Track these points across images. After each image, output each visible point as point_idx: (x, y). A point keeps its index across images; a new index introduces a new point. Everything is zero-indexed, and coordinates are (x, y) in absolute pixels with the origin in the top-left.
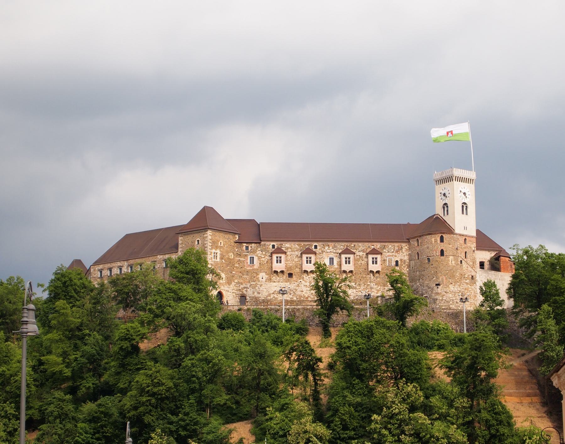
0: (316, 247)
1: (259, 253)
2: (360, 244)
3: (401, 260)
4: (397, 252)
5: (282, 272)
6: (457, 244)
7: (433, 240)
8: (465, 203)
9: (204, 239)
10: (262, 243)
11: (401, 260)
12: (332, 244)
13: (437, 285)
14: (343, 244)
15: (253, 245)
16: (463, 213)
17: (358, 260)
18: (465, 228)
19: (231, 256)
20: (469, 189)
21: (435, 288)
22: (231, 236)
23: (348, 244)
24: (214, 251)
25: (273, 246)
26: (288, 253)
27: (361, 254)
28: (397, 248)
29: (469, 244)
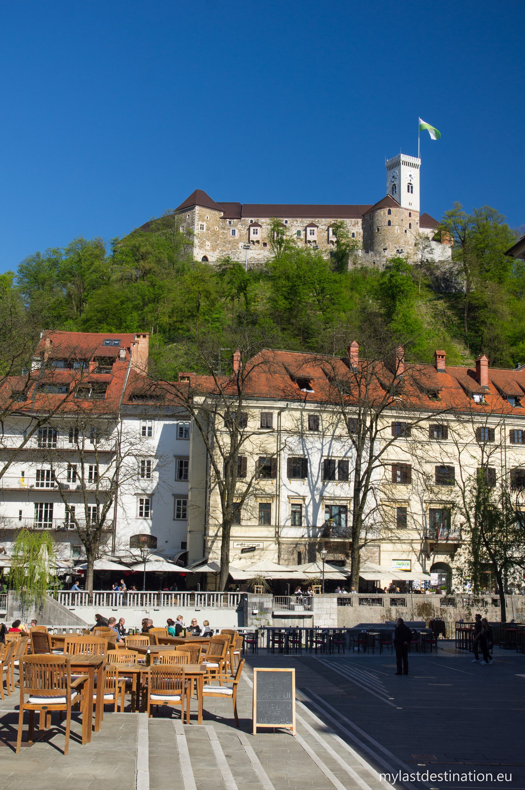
0: (286, 222)
1: (239, 226)
2: (323, 220)
3: (357, 232)
4: (353, 225)
5: (258, 242)
6: (403, 217)
7: (382, 213)
8: (410, 184)
9: (193, 213)
10: (242, 219)
11: (357, 232)
12: (299, 220)
13: (384, 249)
14: (309, 219)
15: (235, 220)
16: (408, 191)
17: (321, 232)
18: (410, 204)
19: (216, 228)
20: (416, 173)
21: (383, 252)
22: (217, 213)
23: (313, 219)
24: (200, 223)
25: (251, 221)
26: (263, 227)
27: (324, 227)
28: (353, 223)
29: (413, 217)
